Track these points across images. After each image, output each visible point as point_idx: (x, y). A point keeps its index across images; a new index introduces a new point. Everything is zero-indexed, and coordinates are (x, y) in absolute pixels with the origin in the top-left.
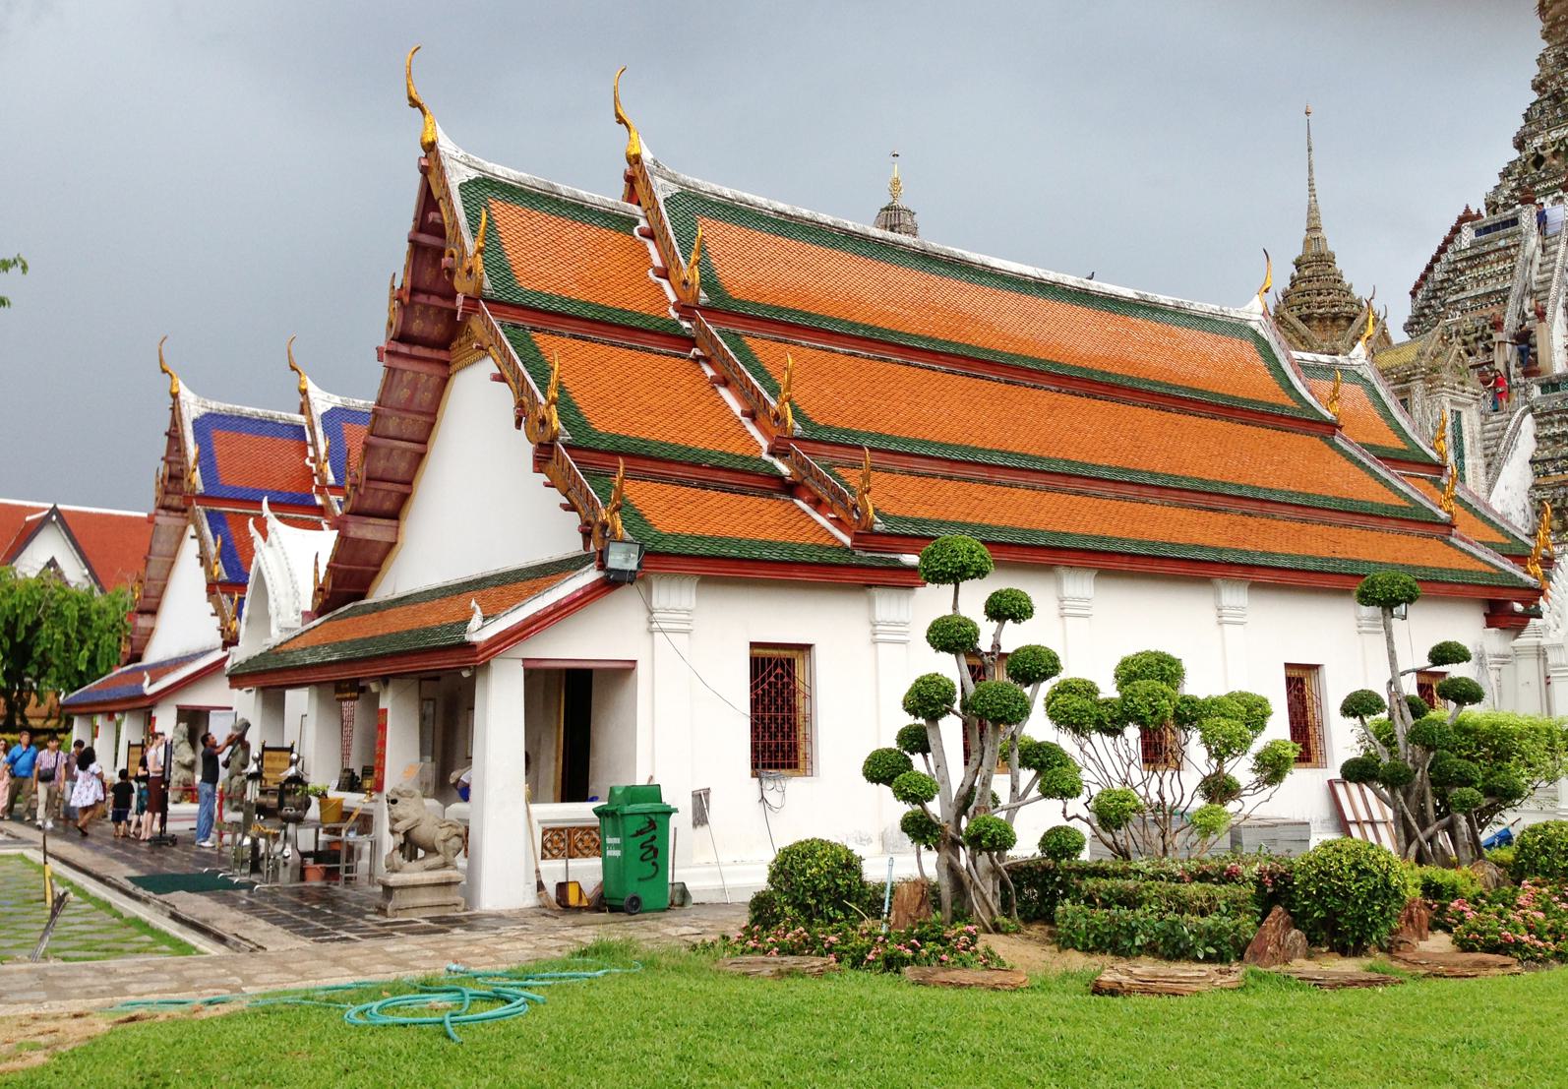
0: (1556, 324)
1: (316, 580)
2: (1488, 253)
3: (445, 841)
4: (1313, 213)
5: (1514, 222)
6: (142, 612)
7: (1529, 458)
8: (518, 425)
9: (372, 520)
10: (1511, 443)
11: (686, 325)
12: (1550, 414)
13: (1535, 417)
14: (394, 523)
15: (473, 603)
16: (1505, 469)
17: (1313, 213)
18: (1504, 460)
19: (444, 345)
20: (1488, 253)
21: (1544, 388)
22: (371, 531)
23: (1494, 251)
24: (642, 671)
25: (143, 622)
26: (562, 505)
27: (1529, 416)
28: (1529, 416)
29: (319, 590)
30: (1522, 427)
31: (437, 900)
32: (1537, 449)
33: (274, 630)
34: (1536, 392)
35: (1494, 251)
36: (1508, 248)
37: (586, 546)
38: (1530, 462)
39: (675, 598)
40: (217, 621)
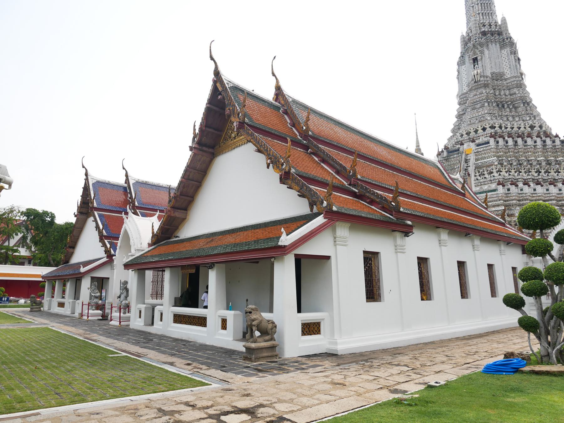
1: (153, 232)
3: (272, 329)
4: (418, 142)
5: (488, 143)
6: (70, 247)
8: (268, 167)
9: (179, 211)
11: (305, 142)
14: (185, 212)
15: (283, 229)
17: (418, 142)
19: (213, 147)
22: (178, 214)
24: (333, 259)
25: (71, 250)
26: (298, 195)
29: (154, 235)
31: (270, 354)
33: (133, 251)
37: (312, 210)
39: (343, 231)
40: (103, 249)
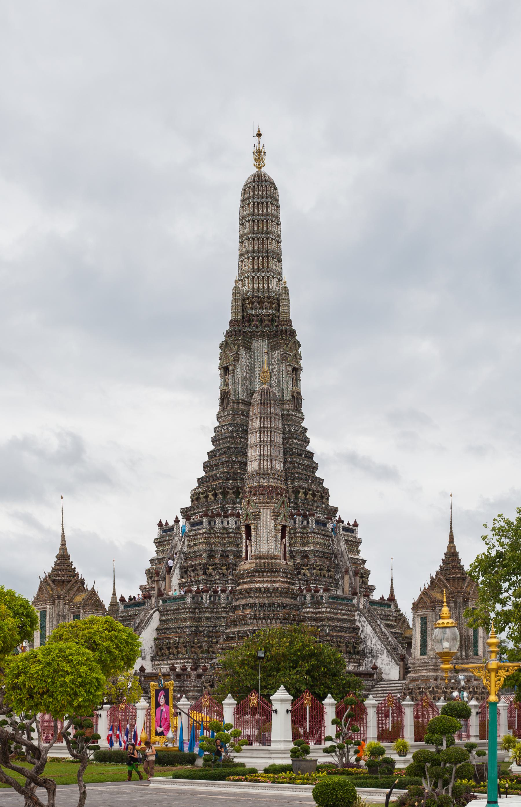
0: (175, 574)
2: (164, 541)
7: (155, 627)
10: (148, 623)
12: (163, 612)
13: (159, 612)
16: (143, 633)
18: (143, 629)
20: (164, 541)
21: (163, 601)
23: (166, 541)
27: (157, 612)
28: (157, 612)
30: (153, 617)
32: (160, 625)
34: (161, 603)
35: (166, 541)
36: (169, 540)
38: (156, 629)
